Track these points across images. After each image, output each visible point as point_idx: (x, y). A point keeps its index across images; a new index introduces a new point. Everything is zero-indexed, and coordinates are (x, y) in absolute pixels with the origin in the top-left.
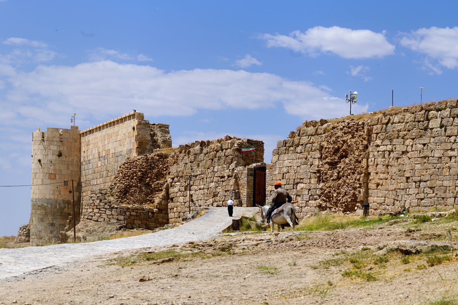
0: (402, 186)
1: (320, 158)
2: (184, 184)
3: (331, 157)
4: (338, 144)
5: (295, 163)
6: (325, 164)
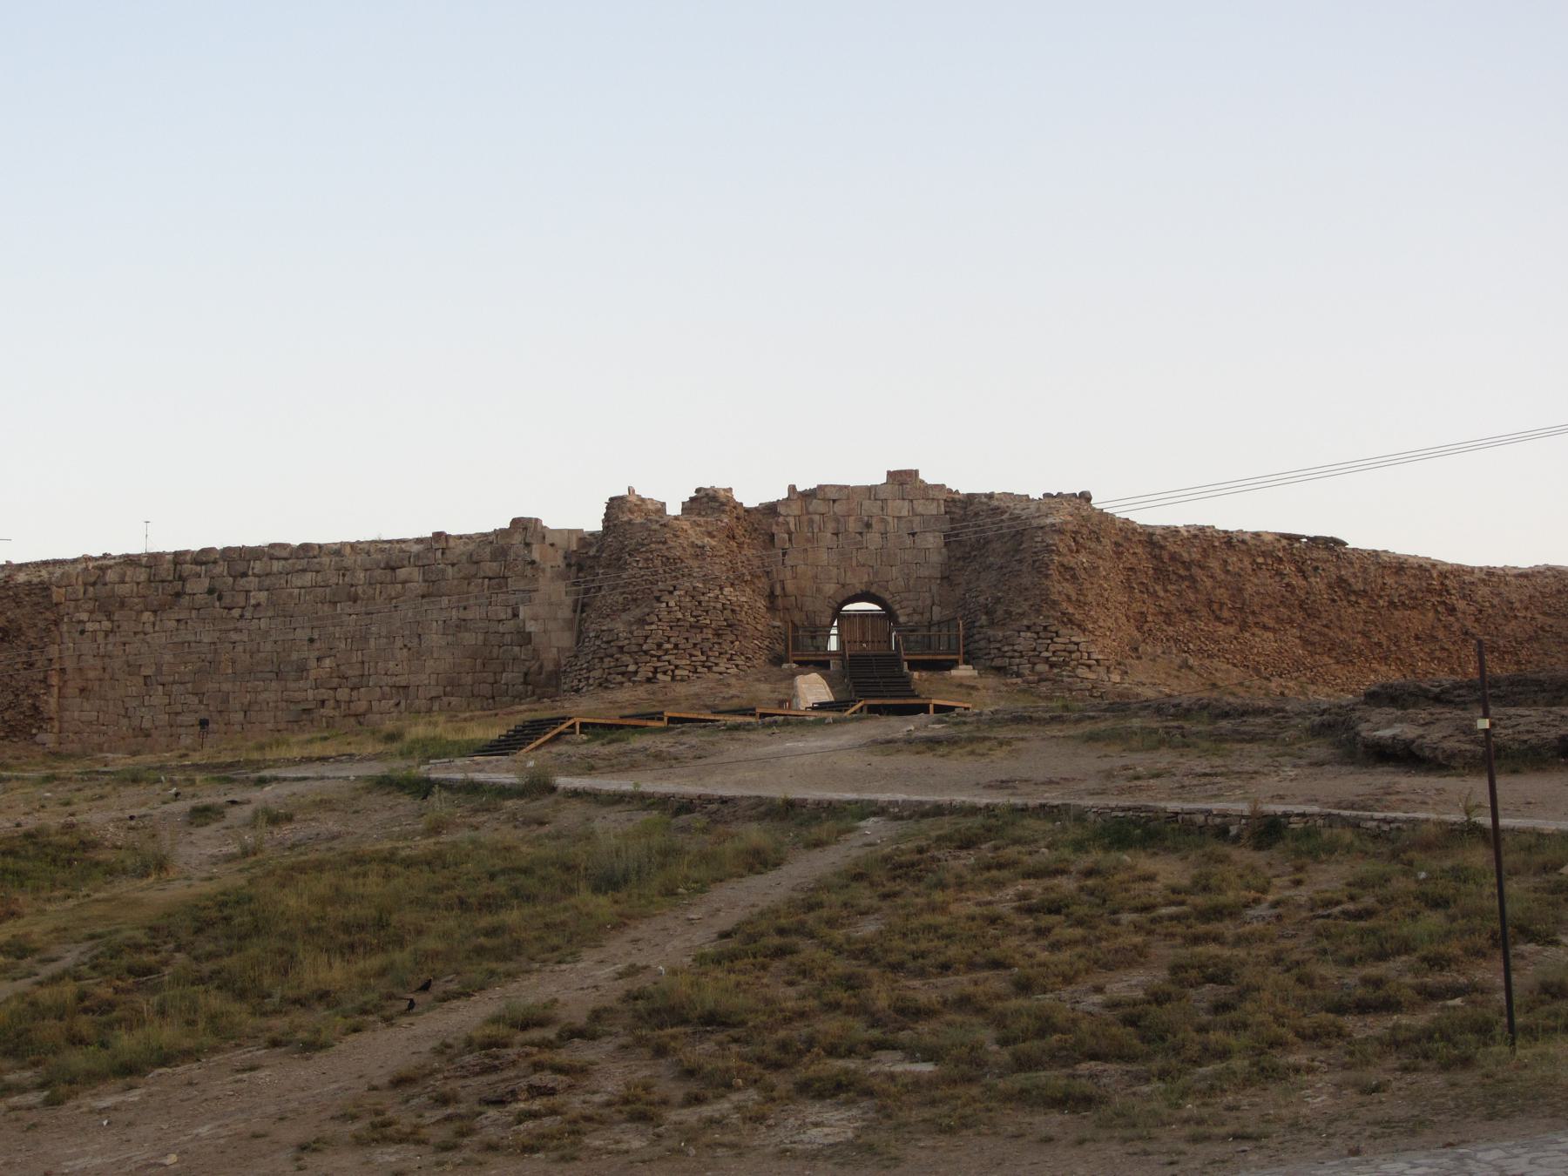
0: (133, 691)
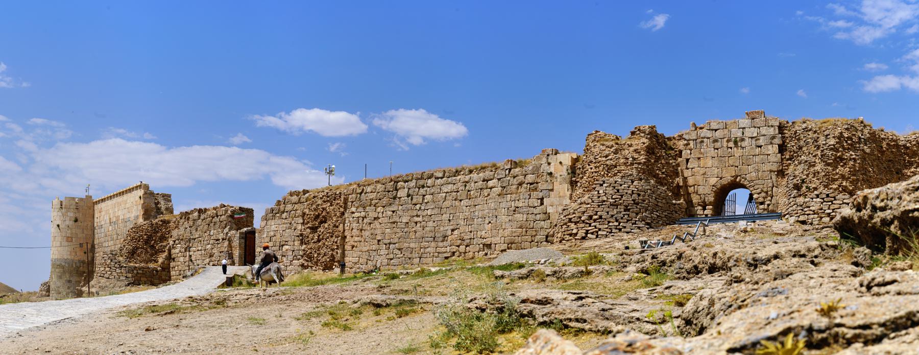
0: (374, 247)
1: (303, 224)
2: (184, 246)
3: (312, 222)
4: (319, 212)
5: (281, 228)
6: (307, 228)
